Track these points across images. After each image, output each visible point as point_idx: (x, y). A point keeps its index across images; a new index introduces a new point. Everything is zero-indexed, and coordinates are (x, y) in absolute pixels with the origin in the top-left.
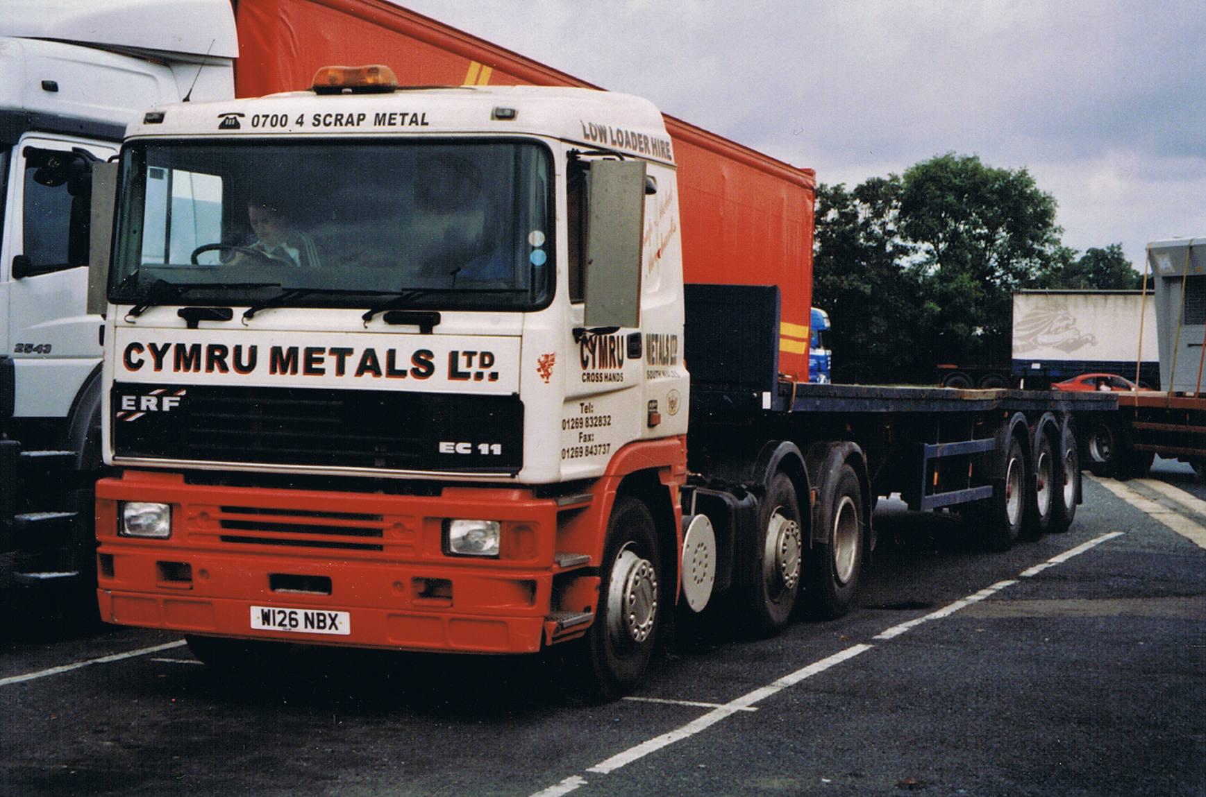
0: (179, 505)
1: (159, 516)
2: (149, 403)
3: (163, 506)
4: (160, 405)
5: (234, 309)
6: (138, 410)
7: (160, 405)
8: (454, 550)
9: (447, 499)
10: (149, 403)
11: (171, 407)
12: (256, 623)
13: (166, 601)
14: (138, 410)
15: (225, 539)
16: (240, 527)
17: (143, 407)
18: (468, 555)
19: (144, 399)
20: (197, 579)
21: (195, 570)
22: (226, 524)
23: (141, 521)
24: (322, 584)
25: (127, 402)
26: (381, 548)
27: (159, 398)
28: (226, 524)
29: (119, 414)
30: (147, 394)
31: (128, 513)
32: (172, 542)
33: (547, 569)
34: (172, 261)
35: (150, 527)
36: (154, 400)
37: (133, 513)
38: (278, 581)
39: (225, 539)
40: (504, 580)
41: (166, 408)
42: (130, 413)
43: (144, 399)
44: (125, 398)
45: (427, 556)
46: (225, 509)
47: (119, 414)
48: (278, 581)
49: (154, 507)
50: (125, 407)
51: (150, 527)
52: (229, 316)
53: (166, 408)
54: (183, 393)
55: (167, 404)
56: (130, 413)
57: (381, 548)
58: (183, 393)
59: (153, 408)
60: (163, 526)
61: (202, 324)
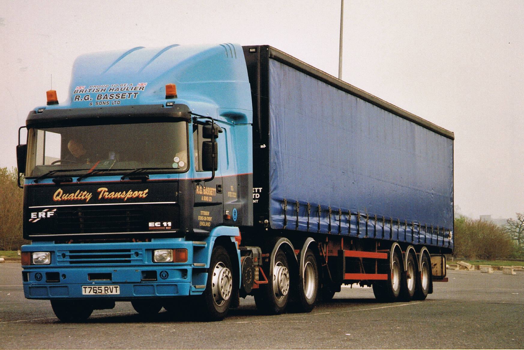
0: (54, 252)
2: (42, 215)
3: (47, 253)
4: (46, 215)
6: (38, 218)
7: (46, 215)
9: (154, 242)
10: (42, 215)
12: (84, 293)
13: (50, 287)
15: (71, 262)
16: (77, 258)
17: (40, 216)
18: (162, 263)
19: (40, 213)
20: (61, 278)
21: (61, 275)
22: (71, 257)
24: (108, 276)
25: (33, 215)
26: (129, 261)
27: (46, 212)
28: (71, 257)
29: (30, 220)
32: (51, 265)
33: (191, 265)
34: (45, 164)
35: (43, 261)
36: (44, 214)
38: (93, 276)
39: (71, 262)
40: (175, 269)
41: (48, 216)
42: (35, 219)
43: (40, 213)
44: (32, 214)
45: (146, 263)
46: (71, 252)
47: (30, 220)
48: (93, 276)
50: (32, 217)
51: (43, 261)
54: (55, 210)
55: (49, 214)
56: (35, 219)
57: (129, 261)
58: (55, 210)
59: (44, 216)
60: (47, 261)
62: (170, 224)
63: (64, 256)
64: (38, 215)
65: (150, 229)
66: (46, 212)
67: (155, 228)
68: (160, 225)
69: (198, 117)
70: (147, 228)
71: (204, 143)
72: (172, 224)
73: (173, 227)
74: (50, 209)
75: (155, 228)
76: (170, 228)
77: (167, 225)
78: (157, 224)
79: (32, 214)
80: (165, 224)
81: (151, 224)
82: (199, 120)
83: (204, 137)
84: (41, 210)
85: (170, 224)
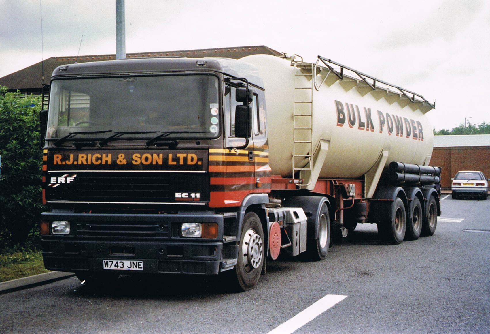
1: (66, 226)
2: (62, 180)
4: (66, 181)
5: (96, 142)
6: (57, 183)
7: (66, 181)
8: (184, 235)
10: (62, 180)
11: (70, 182)
14: (57, 183)
17: (59, 182)
19: (59, 178)
23: (58, 228)
25: (53, 180)
27: (66, 178)
29: (49, 185)
30: (61, 177)
31: (53, 226)
36: (64, 179)
37: (55, 225)
39: (91, 234)
41: (68, 182)
42: (54, 184)
43: (59, 178)
44: (52, 178)
47: (49, 185)
49: (63, 223)
50: (52, 182)
51: (62, 231)
52: (94, 145)
53: (68, 182)
54: (75, 176)
55: (69, 180)
56: (54, 184)
58: (75, 176)
60: (68, 230)
61: (83, 148)
62: (198, 195)
63: (83, 226)
64: (57, 180)
65: (176, 200)
66: (66, 178)
67: (181, 200)
68: (187, 197)
69: (231, 78)
70: (174, 200)
71: (238, 107)
72: (201, 195)
73: (201, 199)
74: (70, 175)
75: (182, 200)
76: (197, 200)
77: (196, 196)
78: (185, 195)
79: (52, 178)
80: (193, 195)
81: (178, 195)
82: (232, 81)
83: (238, 99)
84: (60, 175)
85: (198, 195)
